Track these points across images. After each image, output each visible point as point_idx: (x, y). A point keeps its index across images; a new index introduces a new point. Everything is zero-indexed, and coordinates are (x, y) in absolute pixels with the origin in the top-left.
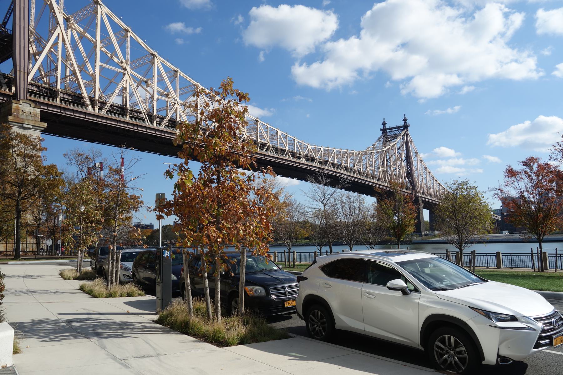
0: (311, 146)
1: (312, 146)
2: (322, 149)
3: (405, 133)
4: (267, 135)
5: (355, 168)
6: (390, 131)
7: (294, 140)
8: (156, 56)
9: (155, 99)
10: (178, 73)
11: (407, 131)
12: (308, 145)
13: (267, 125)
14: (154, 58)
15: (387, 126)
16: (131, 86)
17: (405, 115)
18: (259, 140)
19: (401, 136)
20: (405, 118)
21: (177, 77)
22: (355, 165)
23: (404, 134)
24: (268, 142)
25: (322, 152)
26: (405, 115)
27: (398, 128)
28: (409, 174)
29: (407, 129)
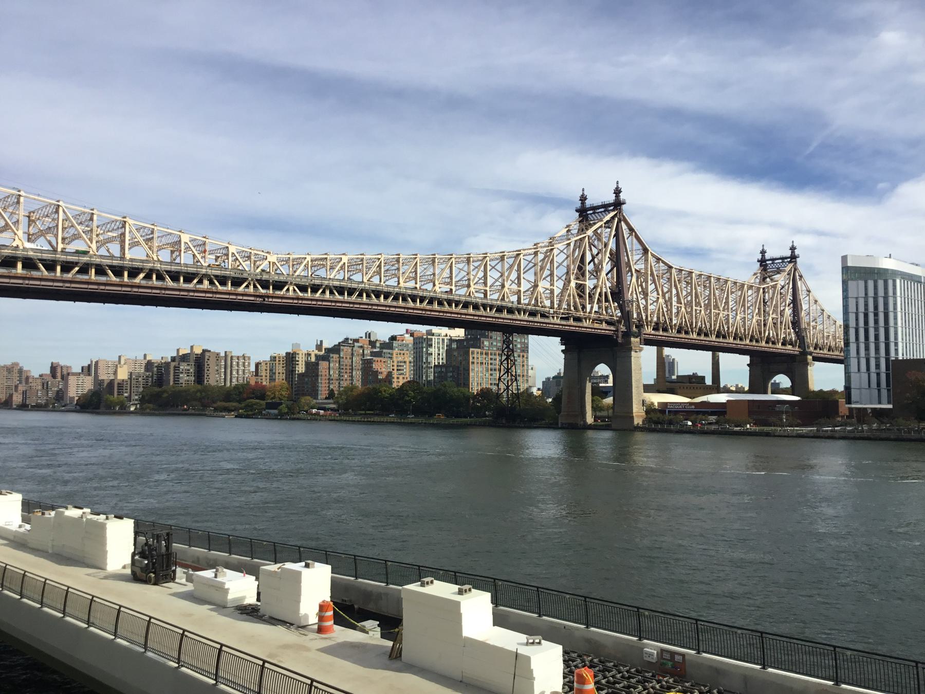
3: (616, 215)
5: (437, 288)
6: (591, 212)
17: (617, 183)
23: (613, 218)
26: (617, 183)
27: (606, 207)
28: (618, 294)
29: (620, 209)
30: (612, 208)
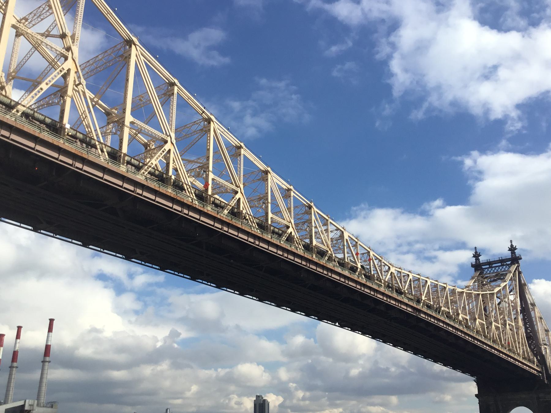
0: (394, 268)
1: (396, 269)
2: (411, 277)
4: (328, 239)
7: (369, 252)
8: (135, 45)
9: (127, 123)
10: (176, 88)
11: (518, 266)
12: (390, 265)
13: (327, 218)
14: (131, 47)
15: (482, 259)
16: (77, 86)
17: (511, 242)
18: (315, 242)
19: (512, 274)
20: (512, 246)
21: (173, 94)
22: (460, 312)
23: (515, 271)
24: (330, 249)
25: (410, 281)
26: (511, 242)
30: (509, 263)
